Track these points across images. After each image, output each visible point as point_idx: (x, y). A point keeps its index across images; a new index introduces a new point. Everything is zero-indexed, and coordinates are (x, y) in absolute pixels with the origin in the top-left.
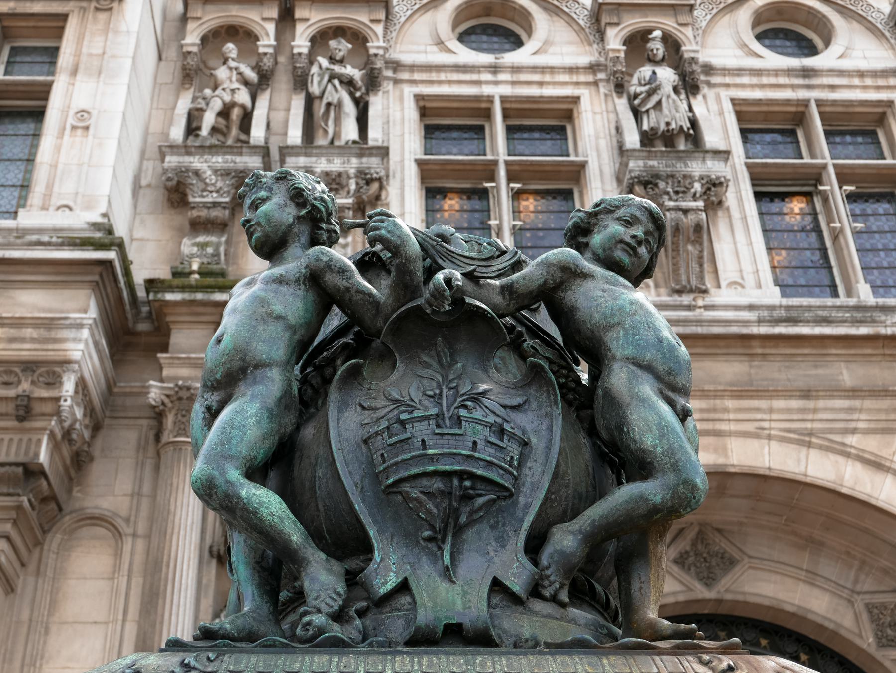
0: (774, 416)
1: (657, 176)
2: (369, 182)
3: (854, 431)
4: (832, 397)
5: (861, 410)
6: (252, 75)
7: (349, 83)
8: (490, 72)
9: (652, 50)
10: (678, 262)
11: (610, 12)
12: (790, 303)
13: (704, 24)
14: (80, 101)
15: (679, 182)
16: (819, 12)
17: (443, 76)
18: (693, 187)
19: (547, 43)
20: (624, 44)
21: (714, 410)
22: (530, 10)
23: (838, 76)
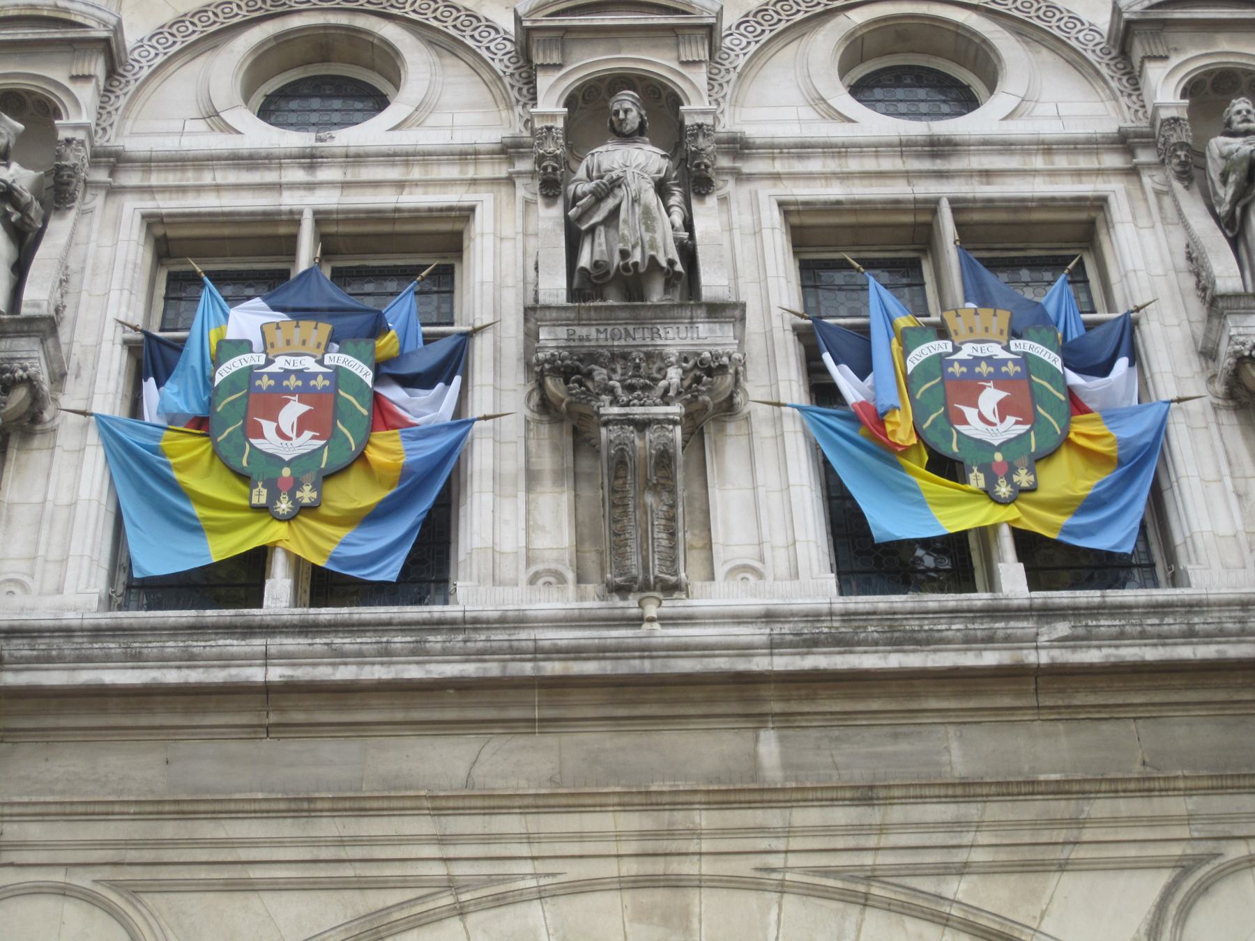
0: (795, 844)
1: (592, 357)
3: (963, 870)
4: (921, 799)
5: (979, 826)
8: (302, 166)
9: (617, 113)
10: (623, 530)
11: (547, 44)
12: (852, 607)
13: (742, 61)
15: (637, 367)
16: (975, 33)
17: (207, 178)
18: (664, 377)
19: (423, 108)
20: (565, 105)
21: (670, 834)
22: (398, 46)
23: (1000, 153)
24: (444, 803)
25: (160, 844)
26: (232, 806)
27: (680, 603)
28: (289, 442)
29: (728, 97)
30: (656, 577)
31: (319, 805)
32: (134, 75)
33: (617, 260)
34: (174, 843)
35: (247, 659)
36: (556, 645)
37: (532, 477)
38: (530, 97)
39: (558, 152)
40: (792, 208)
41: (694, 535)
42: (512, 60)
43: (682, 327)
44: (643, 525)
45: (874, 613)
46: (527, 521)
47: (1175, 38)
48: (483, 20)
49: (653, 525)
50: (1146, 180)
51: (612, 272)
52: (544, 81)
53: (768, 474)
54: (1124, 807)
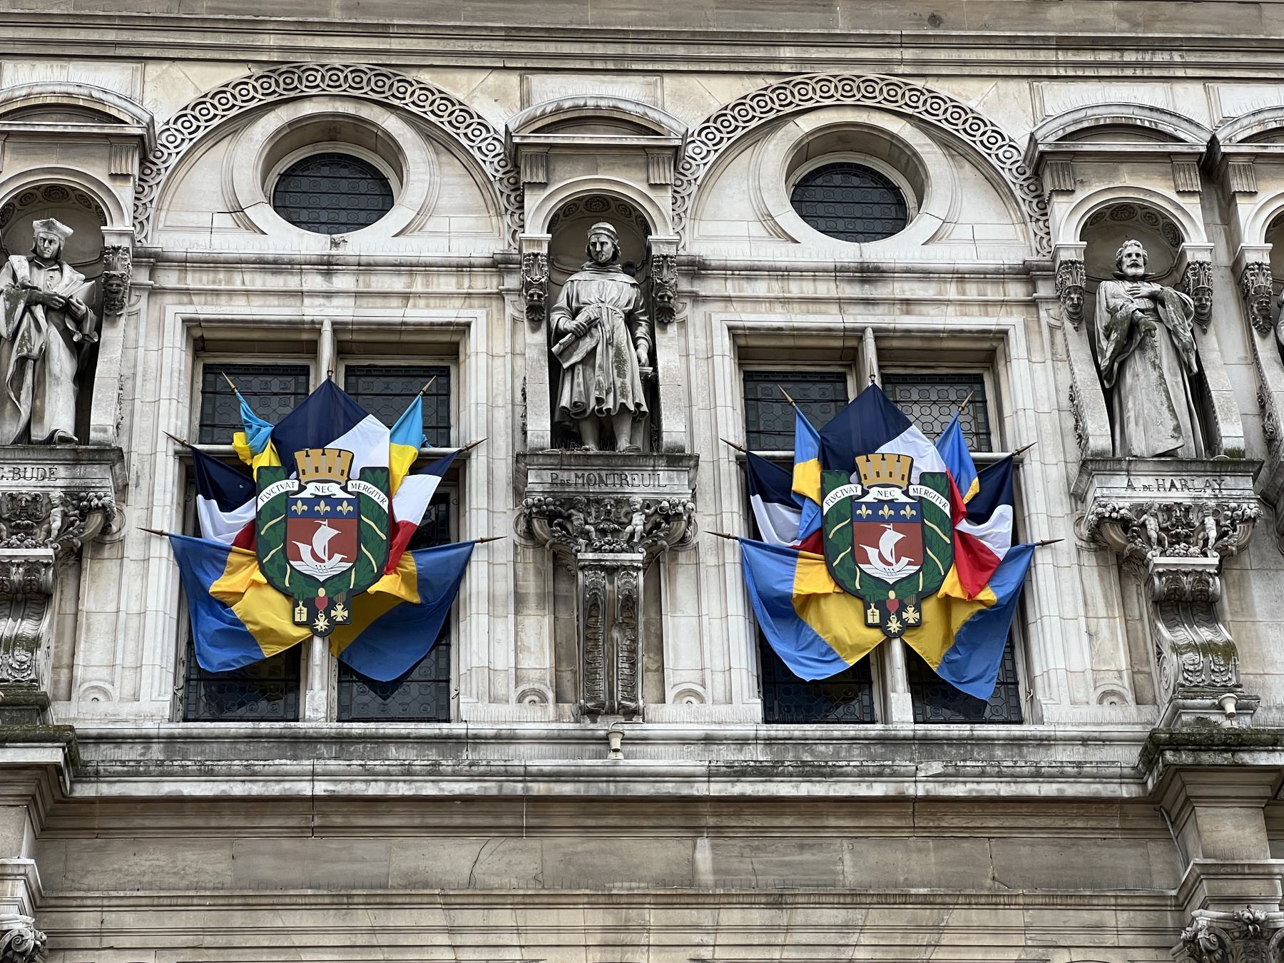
0: (722, 939)
1: (571, 503)
2: (85, 513)
5: (862, 929)
7: (61, 310)
8: (320, 272)
9: (594, 244)
10: (594, 659)
12: (773, 733)
13: (702, 172)
15: (609, 512)
16: (908, 146)
17: (237, 282)
18: (630, 523)
21: (625, 928)
22: (400, 140)
23: (920, 280)
24: (453, 900)
25: (230, 931)
26: (287, 900)
27: (638, 727)
28: (322, 564)
29: (689, 211)
30: (619, 704)
31: (356, 900)
32: (164, 162)
33: (593, 403)
34: (241, 930)
35: (299, 775)
36: (541, 770)
37: (519, 600)
38: (517, 205)
39: (543, 280)
40: (740, 332)
41: (649, 658)
42: (501, 163)
43: (646, 474)
44: (611, 656)
45: (790, 739)
46: (516, 642)
47: (1082, 168)
48: (475, 116)
49: (618, 656)
50: (1043, 314)
51: (589, 411)
52: (532, 200)
53: (711, 604)
54: (977, 917)
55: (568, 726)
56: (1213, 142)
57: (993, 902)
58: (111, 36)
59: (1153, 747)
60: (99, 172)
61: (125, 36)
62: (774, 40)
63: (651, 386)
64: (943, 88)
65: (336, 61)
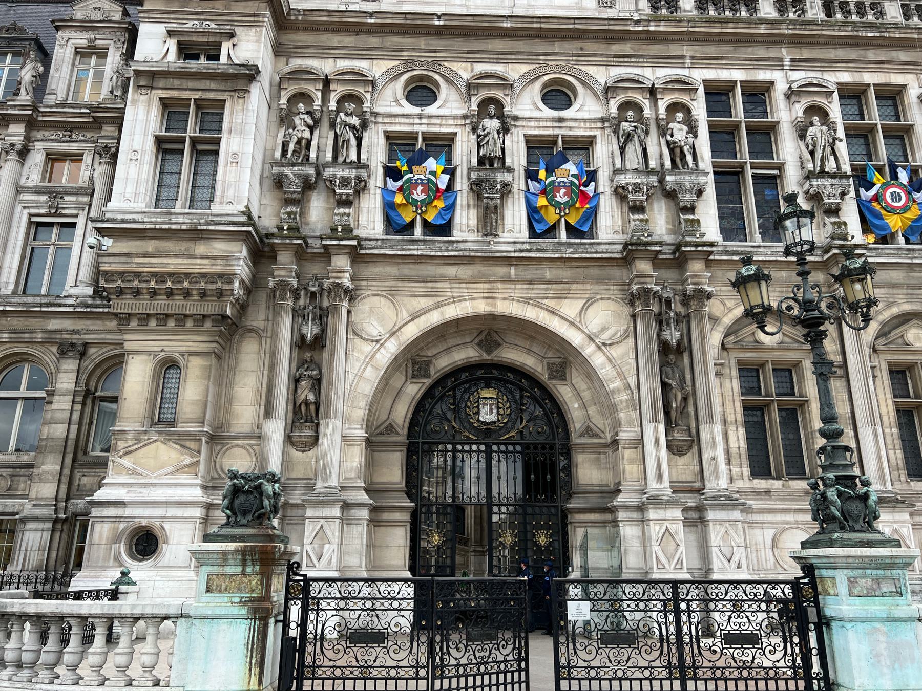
1: (482, 181)
2: (360, 182)
3: (547, 298)
6: (310, 122)
7: (353, 127)
14: (234, 148)
21: (493, 288)
37: (469, 206)
47: (618, 91)
52: (473, 99)
54: (579, 287)
55: (480, 239)
56: (653, 84)
57: (583, 283)
58: (364, 52)
59: (626, 245)
60: (362, 90)
61: (368, 52)
62: (539, 54)
63: (503, 150)
64: (582, 68)
65: (422, 59)
